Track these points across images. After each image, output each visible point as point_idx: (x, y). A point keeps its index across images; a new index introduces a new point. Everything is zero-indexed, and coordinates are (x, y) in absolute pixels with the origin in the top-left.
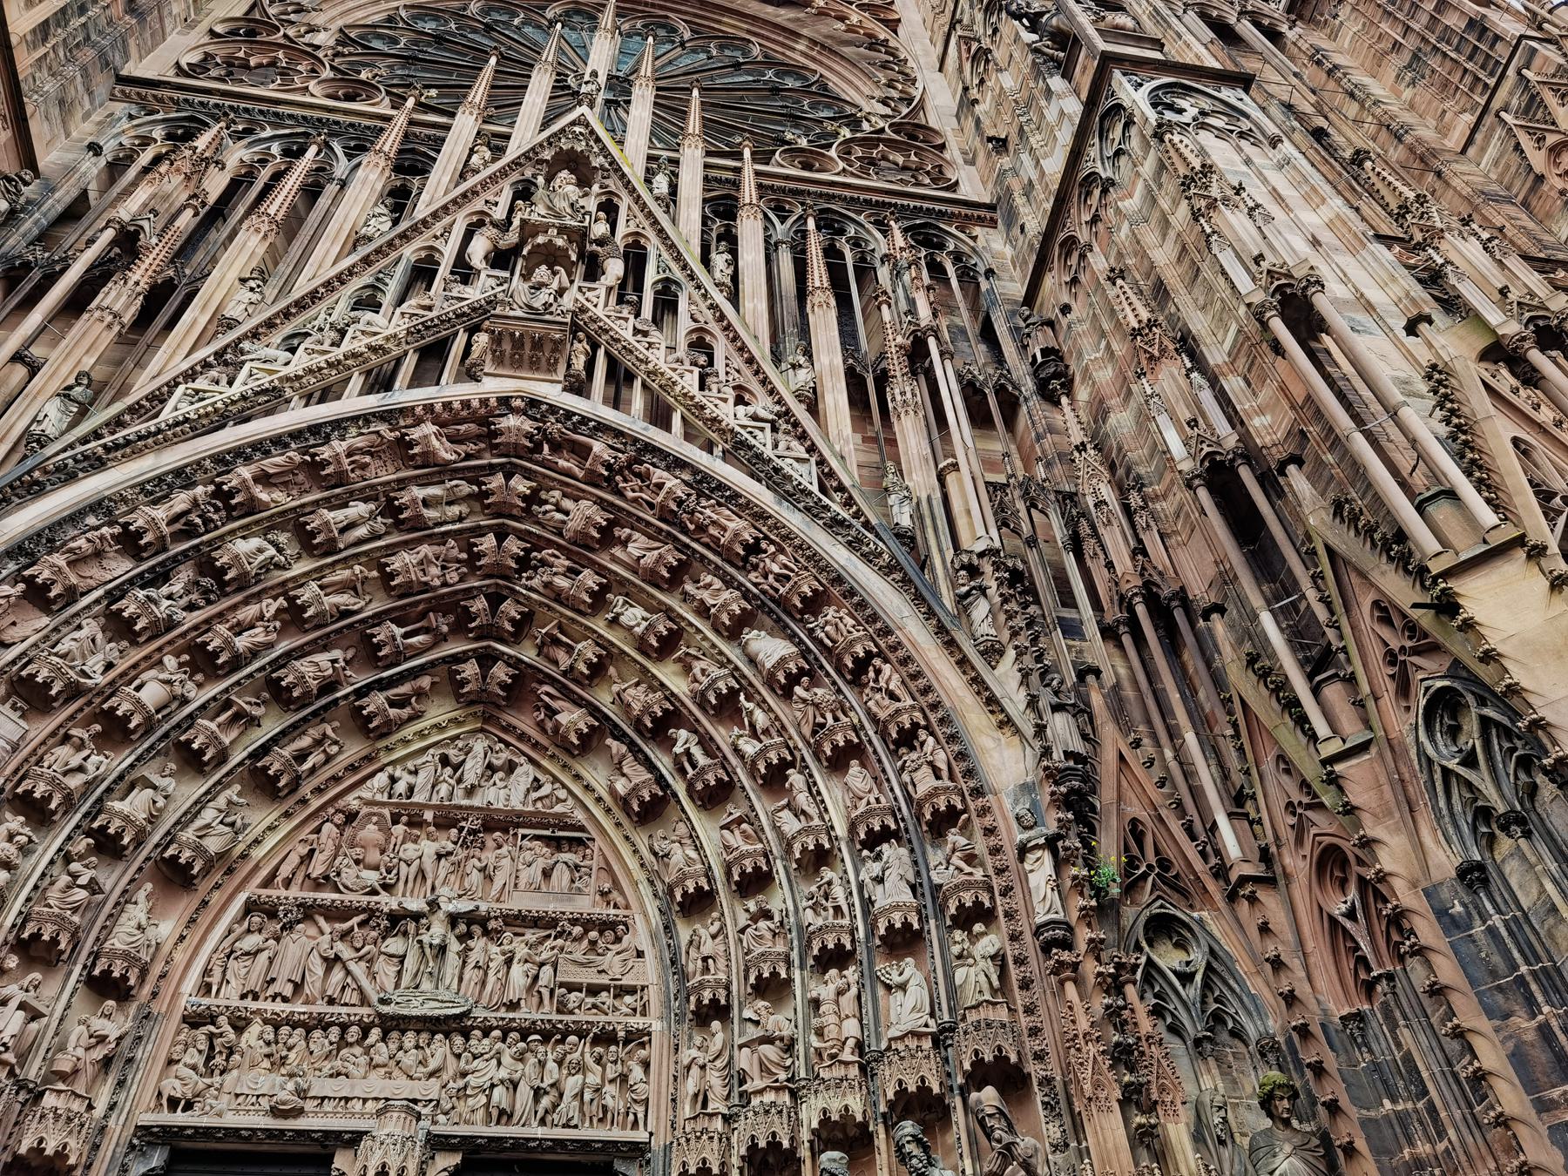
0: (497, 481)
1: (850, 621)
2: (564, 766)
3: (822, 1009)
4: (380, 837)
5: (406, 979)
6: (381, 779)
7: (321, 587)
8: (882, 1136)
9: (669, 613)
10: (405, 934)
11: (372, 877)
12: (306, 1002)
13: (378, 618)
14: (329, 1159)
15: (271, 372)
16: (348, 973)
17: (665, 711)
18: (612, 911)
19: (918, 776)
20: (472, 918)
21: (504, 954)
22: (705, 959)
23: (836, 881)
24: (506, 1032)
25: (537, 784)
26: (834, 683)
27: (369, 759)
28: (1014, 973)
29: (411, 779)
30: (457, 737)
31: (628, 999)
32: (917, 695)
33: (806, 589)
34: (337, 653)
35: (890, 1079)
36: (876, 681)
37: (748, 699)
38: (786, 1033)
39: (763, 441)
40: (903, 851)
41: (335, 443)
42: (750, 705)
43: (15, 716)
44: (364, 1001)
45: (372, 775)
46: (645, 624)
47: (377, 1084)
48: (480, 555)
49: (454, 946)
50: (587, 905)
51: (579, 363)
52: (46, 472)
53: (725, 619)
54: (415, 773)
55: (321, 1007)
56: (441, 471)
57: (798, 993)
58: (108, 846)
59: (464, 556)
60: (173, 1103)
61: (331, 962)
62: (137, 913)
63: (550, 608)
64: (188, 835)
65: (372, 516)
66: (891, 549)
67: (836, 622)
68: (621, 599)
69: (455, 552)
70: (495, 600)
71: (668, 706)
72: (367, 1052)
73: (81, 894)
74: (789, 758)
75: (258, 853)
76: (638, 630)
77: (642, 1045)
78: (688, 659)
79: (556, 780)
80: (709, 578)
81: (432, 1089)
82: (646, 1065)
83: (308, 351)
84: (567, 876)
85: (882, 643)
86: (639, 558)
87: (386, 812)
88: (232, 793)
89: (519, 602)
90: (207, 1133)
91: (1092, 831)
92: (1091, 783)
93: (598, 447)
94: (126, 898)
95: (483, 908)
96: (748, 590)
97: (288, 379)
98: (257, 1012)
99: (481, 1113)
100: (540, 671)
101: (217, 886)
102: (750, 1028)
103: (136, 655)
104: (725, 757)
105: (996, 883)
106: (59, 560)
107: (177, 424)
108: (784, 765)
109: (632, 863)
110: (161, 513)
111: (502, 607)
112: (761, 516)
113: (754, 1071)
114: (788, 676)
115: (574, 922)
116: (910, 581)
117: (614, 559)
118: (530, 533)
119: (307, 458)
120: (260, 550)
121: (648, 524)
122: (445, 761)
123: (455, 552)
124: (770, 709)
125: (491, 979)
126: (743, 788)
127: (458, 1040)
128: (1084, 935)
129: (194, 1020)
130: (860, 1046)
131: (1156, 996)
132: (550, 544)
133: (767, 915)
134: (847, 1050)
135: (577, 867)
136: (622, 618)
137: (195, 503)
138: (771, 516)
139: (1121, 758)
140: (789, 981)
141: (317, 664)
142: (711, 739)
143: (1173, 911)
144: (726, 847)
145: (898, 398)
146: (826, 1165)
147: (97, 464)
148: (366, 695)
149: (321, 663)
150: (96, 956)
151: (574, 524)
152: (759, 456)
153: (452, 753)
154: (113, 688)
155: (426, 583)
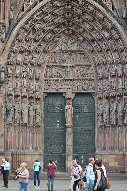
0: (66, 7)
1: (116, 33)
4: (59, 55)
6: (58, 47)
9: (92, 26)
12: (56, 77)
13: (54, 28)
16: (60, 74)
17: (93, 39)
20: (72, 66)
23: (114, 67)
24: (78, 80)
25: (77, 46)
27: (56, 45)
29: (61, 47)
30: (66, 39)
31: (92, 75)
33: (110, 27)
36: (119, 42)
37: (104, 40)
38: (108, 84)
42: (104, 41)
44: (62, 77)
48: (66, 17)
49: (71, 70)
53: (100, 29)
55: (58, 78)
56: (59, 7)
59: (63, 17)
60: (46, 89)
67: (114, 32)
68: (86, 23)
72: (64, 83)
75: (46, 60)
76: (89, 28)
79: (80, 45)
81: (71, 87)
82: (94, 83)
87: (59, 52)
88: (42, 54)
106: (20, 36)
108: (108, 50)
110: (28, 26)
111: (70, 23)
112: (104, 14)
113: (105, 88)
114: (108, 39)
115: (84, 66)
117: (84, 17)
119: (42, 11)
120: (39, 25)
122: (65, 42)
125: (76, 73)
127: (73, 81)
129: (45, 80)
130: (116, 87)
132: (75, 15)
134: (114, 88)
135: (84, 57)
138: (105, 15)
140: (109, 78)
149: (48, 36)
151: (78, 13)
153: (66, 42)
154: (28, 48)
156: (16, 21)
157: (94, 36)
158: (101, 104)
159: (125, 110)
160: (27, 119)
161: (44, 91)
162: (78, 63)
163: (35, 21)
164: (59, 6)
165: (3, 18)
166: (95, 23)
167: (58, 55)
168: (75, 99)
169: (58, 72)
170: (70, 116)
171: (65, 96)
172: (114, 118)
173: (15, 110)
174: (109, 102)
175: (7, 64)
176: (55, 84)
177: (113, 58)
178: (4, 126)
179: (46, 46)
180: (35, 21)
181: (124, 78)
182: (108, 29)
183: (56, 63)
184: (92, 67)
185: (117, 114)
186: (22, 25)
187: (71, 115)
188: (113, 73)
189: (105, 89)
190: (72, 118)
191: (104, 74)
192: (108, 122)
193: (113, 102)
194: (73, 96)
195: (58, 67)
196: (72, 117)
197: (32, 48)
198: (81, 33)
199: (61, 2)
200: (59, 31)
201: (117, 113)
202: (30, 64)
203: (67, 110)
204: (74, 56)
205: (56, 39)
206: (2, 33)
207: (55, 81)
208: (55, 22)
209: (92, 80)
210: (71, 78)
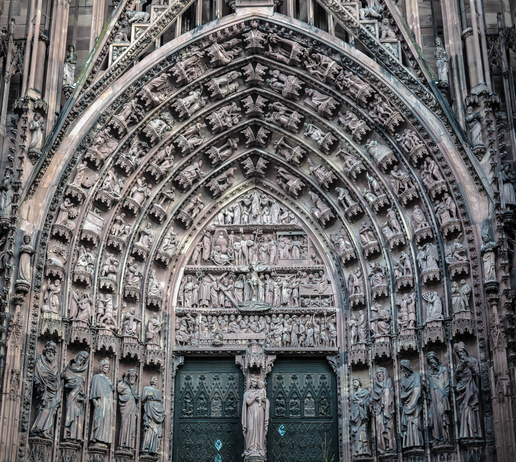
3: (402, 310)
7: (185, 136)
8: (422, 355)
9: (332, 131)
14: (234, 358)
23: (407, 258)
34: (196, 165)
35: (426, 337)
37: (370, 175)
40: (435, 247)
41: (178, 64)
42: (371, 178)
43: (98, 215)
46: (322, 139)
53: (359, 136)
57: (392, 302)
61: (219, 291)
63: (279, 131)
70: (255, 128)
71: (335, 177)
74: (388, 203)
78: (343, 155)
83: (157, 10)
86: (318, 106)
89: (265, 129)
96: (369, 121)
97: (152, 31)
100: (278, 161)
101: (174, 267)
103: (129, 182)
104: (360, 202)
108: (386, 206)
118: (267, 94)
124: (380, 180)
126: (369, 216)
130: (415, 323)
134: (411, 325)
136: (312, 136)
141: (190, 172)
142: (354, 193)
146: (403, 364)
147: (92, 97)
148: (209, 181)
155: (226, 126)
170: (259, 425)
177: (402, 228)
185: (425, 411)
188: (407, 279)
190: (266, 433)
191: (373, 285)
199: (232, 52)
201: (425, 406)
203: (248, 406)
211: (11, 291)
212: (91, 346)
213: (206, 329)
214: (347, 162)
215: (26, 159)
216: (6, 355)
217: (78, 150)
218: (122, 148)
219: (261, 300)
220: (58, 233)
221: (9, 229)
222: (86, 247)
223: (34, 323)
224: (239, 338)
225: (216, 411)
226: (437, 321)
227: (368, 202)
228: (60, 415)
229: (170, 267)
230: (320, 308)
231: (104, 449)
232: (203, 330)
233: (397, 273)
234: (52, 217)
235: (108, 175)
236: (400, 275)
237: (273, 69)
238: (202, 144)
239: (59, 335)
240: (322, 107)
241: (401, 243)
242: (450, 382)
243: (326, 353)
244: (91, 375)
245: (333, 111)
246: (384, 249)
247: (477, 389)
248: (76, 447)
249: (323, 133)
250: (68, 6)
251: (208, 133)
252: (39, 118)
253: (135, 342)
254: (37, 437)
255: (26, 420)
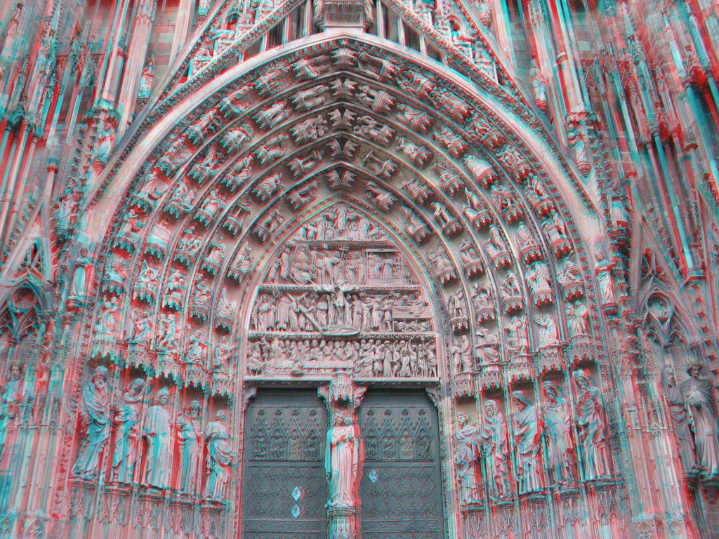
0: (337, 84)
1: (517, 153)
2: (383, 219)
5: (330, 321)
6: (302, 231)
9: (427, 147)
10: (326, 301)
11: (307, 276)
12: (293, 330)
13: (292, 158)
15: (230, 44)
16: (306, 318)
17: (429, 195)
18: (413, 286)
19: (551, 232)
21: (368, 307)
22: (457, 309)
23: (515, 277)
25: (371, 228)
26: (510, 184)
28: (593, 323)
29: (312, 229)
31: (424, 324)
32: (550, 192)
36: (531, 184)
37: (469, 190)
38: (495, 342)
39: (467, 54)
43: (164, 228)
44: (315, 329)
45: (298, 228)
47: (328, 363)
48: (333, 121)
49: (348, 306)
50: (401, 284)
51: (369, 15)
52: (151, 117)
54: (316, 226)
55: (299, 333)
57: (500, 326)
58: (208, 275)
59: (325, 122)
60: (254, 372)
62: (225, 301)
64: (234, 266)
65: (283, 109)
66: (535, 114)
67: (510, 154)
68: (403, 139)
69: (321, 121)
72: (322, 349)
73: (205, 298)
75: (259, 269)
76: (414, 155)
77: (432, 343)
80: (446, 129)
81: (350, 364)
82: (434, 351)
84: (390, 270)
85: (532, 165)
86: (410, 120)
87: (306, 245)
90: (269, 382)
91: (629, 257)
92: (628, 233)
93: (386, 64)
94: (220, 295)
95: (357, 288)
98: (276, 336)
99: (370, 373)
102: (480, 340)
105: (586, 283)
107: (195, 81)
109: (418, 263)
110: (197, 128)
112: (468, 98)
115: (396, 291)
116: (545, 132)
117: (398, 119)
118: (356, 108)
120: (239, 136)
121: (413, 102)
122: (328, 219)
123: (321, 121)
125: (365, 318)
127: (357, 344)
128: (623, 309)
129: (253, 340)
130: (528, 350)
131: (651, 328)
132: (366, 113)
133: (484, 291)
135: (394, 266)
136: (405, 150)
137: (211, 121)
139: (644, 219)
140: (495, 320)
143: (661, 291)
144: (463, 260)
145: (535, 13)
150: (215, 320)
151: (377, 103)
152: (466, 64)
153: (331, 215)
156: (157, 107)
157: (434, 182)
158: (467, 421)
159: (586, 426)
160: (170, 471)
161: (247, 378)
162: (371, 284)
163: (227, 117)
164: (313, 79)
165: (113, 99)
166: (436, 134)
167: (302, 255)
168: (364, 411)
169: (299, 314)
171: (326, 396)
172: (532, 468)
173: (115, 425)
174: (502, 410)
175: (104, 248)
176: (290, 355)
178: (53, 484)
179: (262, 216)
180: (227, 117)
181: (564, 309)
182: (486, 146)
183: (293, 282)
184: (426, 296)
185: (543, 450)
186: (176, 123)
187: (349, 467)
189: (484, 363)
190: (354, 480)
192: (506, 486)
193: (524, 405)
194: (355, 396)
195: (299, 298)
196: (355, 474)
197: (210, 210)
198: (385, 179)
200: (310, 170)
202: (199, 271)
203: (332, 446)
204: (361, 259)
205: (296, 196)
206: (101, 141)
207: (287, 342)
208: (296, 132)
209: (427, 340)
210: (350, 334)
211: (61, 308)
212: (148, 373)
213: (284, 356)
214: (443, 176)
215: (91, 169)
216: (49, 381)
217: (148, 160)
218: (196, 157)
219: (348, 323)
220: (119, 246)
221: (65, 241)
222: (148, 262)
223: (84, 345)
224: (322, 366)
225: (294, 452)
226: (552, 347)
227: (468, 218)
228: (106, 454)
229: (243, 285)
230: (417, 333)
231: (157, 496)
232: (280, 357)
233: (503, 294)
234: (114, 228)
235: (178, 186)
236: (508, 297)
237: (362, 85)
238: (283, 155)
239: (112, 358)
240: (416, 120)
241: (507, 262)
242: (571, 416)
243: (426, 383)
244: (145, 406)
245: (426, 125)
246: (488, 269)
247: (601, 423)
248: (124, 492)
249: (417, 147)
250: (151, 25)
251: (290, 144)
252: (109, 129)
253: (200, 370)
254: (78, 480)
255: (67, 458)
